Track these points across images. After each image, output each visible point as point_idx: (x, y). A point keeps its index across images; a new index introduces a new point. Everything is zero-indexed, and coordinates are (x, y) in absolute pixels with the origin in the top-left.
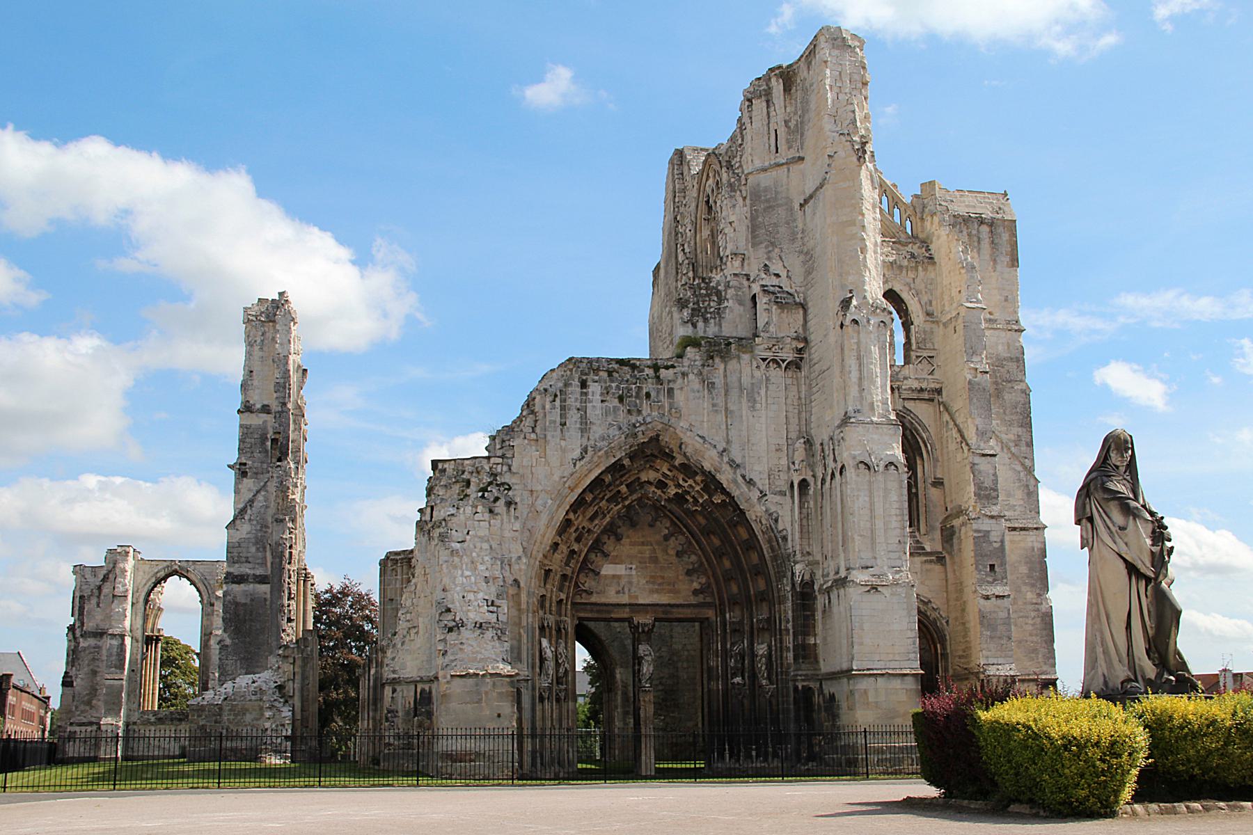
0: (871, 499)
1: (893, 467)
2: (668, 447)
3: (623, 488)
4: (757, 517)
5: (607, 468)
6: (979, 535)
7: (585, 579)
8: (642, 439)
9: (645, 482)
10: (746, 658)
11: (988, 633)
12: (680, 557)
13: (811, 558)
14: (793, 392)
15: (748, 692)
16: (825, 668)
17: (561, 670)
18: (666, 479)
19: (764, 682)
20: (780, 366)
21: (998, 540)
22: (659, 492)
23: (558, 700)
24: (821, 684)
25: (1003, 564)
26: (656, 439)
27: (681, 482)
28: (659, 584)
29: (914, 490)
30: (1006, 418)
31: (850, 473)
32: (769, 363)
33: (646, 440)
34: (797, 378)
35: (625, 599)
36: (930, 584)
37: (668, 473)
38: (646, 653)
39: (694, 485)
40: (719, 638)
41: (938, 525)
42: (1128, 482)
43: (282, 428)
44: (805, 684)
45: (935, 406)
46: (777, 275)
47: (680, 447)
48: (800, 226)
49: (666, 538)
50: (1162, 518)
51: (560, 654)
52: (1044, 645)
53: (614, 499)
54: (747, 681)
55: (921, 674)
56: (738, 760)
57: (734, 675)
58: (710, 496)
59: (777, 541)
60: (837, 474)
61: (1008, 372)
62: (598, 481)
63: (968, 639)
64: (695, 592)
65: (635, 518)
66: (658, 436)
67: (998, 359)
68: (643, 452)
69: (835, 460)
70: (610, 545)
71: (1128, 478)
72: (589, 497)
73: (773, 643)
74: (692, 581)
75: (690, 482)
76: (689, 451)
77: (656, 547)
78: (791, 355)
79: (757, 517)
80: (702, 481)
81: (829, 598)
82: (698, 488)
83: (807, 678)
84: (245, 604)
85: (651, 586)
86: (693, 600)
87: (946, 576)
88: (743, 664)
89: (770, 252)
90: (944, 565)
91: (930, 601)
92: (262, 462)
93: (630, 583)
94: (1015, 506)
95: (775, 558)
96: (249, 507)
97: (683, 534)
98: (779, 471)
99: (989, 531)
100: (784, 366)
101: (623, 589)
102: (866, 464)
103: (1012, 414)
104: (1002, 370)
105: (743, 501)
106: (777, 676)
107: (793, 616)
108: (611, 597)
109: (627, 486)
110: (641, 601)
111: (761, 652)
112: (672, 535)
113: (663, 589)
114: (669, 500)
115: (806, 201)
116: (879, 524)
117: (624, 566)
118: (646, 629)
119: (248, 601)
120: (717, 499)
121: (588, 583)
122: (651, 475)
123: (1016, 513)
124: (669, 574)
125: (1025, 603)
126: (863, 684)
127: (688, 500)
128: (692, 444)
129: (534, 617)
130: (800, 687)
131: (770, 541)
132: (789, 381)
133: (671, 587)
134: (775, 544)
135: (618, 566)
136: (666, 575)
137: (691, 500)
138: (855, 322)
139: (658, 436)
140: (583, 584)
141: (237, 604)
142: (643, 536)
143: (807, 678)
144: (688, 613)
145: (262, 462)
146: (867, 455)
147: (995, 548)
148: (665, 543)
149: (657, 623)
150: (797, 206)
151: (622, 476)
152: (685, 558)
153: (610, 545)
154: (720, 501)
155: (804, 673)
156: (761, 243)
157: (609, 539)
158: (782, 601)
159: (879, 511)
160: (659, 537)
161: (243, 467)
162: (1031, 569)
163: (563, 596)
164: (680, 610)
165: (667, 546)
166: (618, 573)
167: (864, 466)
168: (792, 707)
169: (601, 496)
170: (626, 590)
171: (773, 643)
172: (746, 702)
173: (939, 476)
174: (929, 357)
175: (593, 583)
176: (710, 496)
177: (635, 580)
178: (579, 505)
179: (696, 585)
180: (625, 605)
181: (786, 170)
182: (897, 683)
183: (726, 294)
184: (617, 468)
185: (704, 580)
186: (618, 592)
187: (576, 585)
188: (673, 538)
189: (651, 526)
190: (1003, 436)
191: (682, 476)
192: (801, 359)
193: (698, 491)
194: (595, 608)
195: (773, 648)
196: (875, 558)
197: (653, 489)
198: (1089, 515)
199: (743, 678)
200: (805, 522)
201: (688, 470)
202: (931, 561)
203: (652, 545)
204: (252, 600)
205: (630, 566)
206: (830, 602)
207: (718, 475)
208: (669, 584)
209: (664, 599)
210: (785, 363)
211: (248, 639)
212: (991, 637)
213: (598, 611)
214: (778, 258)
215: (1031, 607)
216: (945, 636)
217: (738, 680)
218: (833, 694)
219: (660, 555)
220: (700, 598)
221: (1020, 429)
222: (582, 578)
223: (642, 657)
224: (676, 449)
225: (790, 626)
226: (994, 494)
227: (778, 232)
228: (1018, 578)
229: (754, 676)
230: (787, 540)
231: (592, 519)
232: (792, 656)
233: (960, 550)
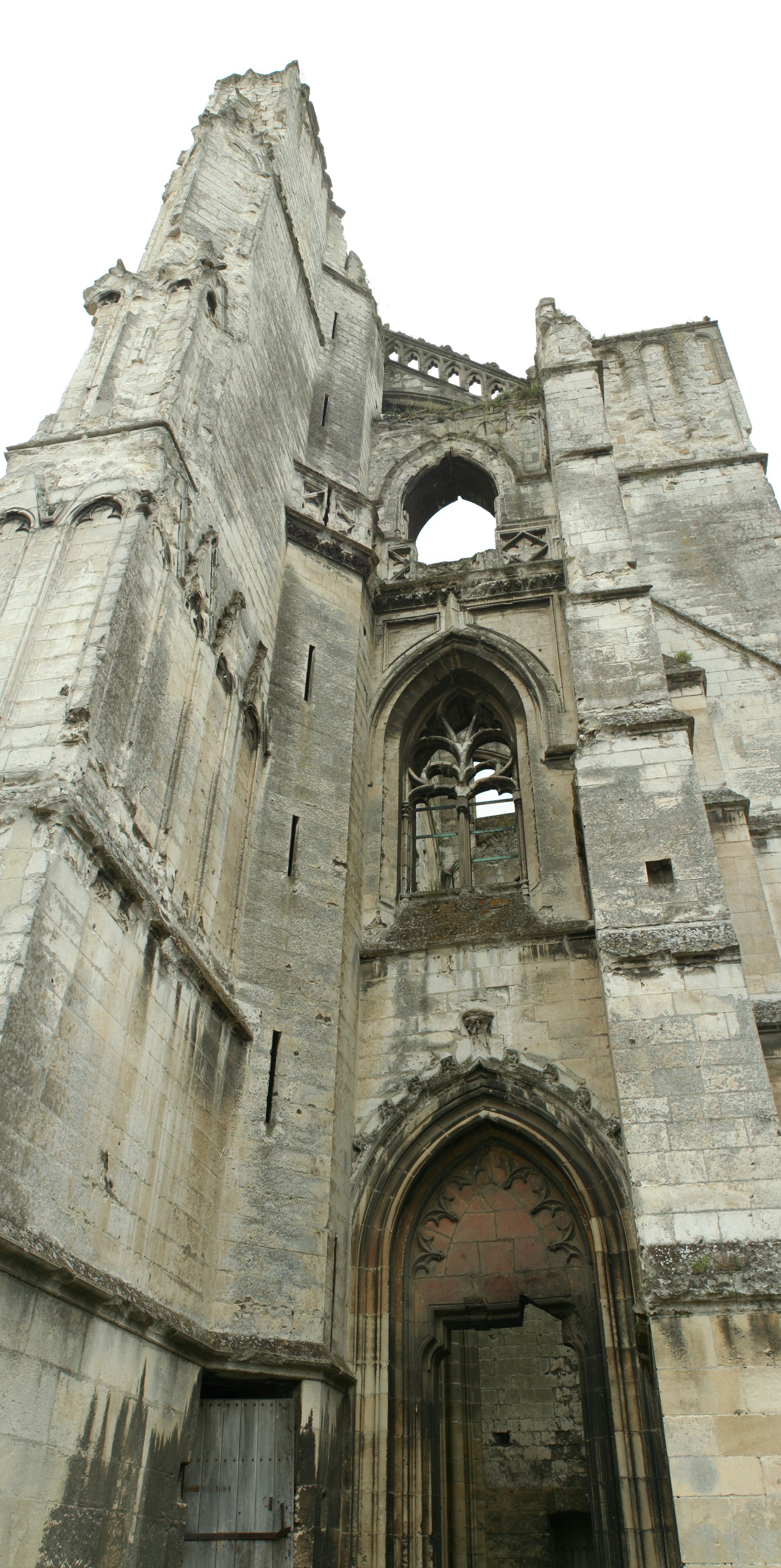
6: (603, 782)
11: (661, 1105)
21: (675, 786)
30: (749, 606)
61: (739, 527)
91: (552, 1071)
99: (634, 770)
104: (723, 527)
212: (672, 1121)
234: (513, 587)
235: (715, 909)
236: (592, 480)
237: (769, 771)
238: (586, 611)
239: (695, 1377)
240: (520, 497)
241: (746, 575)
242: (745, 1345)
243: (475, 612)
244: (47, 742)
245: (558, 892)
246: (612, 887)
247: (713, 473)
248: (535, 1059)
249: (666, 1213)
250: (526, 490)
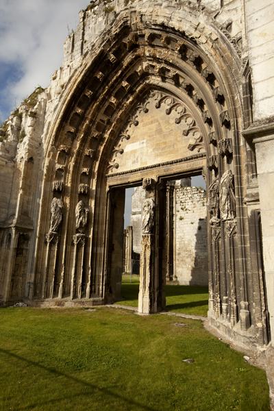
4: (206, 37)
8: (115, 30)
26: (125, 29)
28: (163, 149)
47: (142, 21)
53: (122, 94)
64: (193, 148)
77: (161, 121)
93: (142, 153)
101: (137, 159)
105: (192, 31)
109: (127, 81)
113: (166, 152)
133: (172, 149)
135: (135, 144)
136: (167, 140)
160: (164, 113)
164: (178, 165)
170: (139, 159)
179: (192, 142)
184: (100, 62)
186: (134, 162)
203: (157, 121)
220: (195, 152)
224: (141, 25)
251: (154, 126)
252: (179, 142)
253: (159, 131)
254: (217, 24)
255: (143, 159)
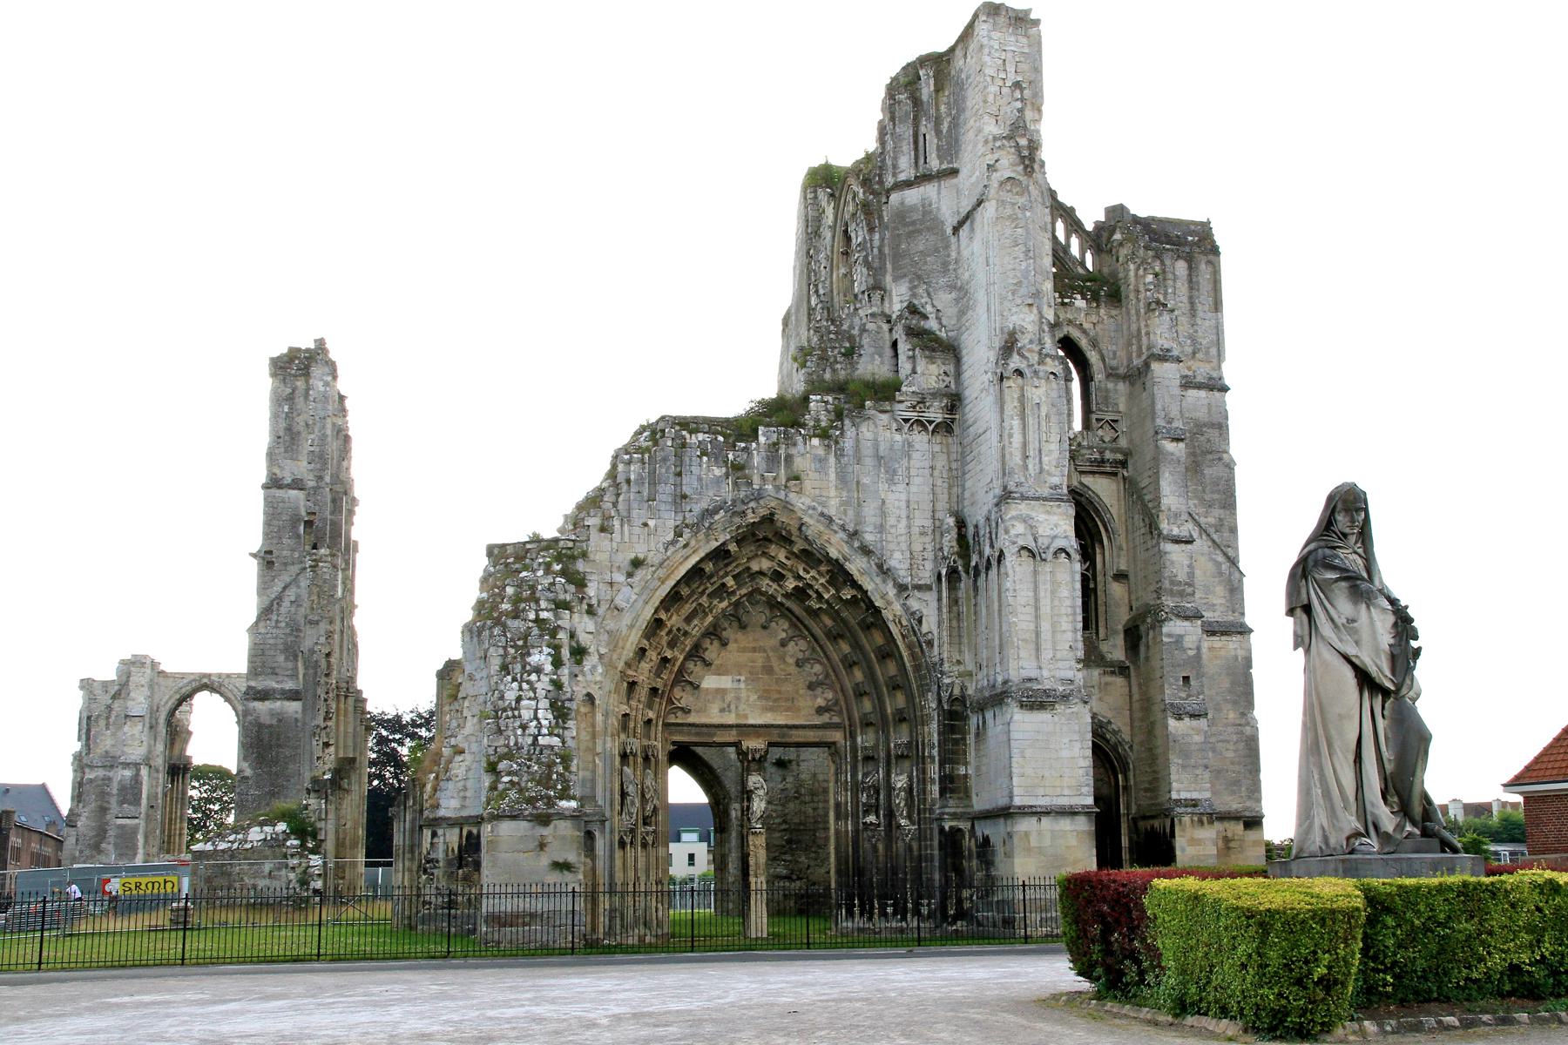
0: (1035, 594)
1: (1063, 555)
2: (785, 529)
3: (730, 582)
5: (707, 555)
7: (682, 694)
8: (751, 518)
9: (757, 572)
10: (881, 791)
11: (1180, 761)
12: (800, 667)
13: (962, 668)
14: (941, 462)
15: (883, 833)
16: (979, 803)
17: (649, 807)
18: (783, 568)
19: (903, 822)
20: (926, 429)
21: (1194, 647)
22: (775, 586)
23: (644, 845)
24: (973, 825)
25: (1200, 676)
26: (769, 519)
27: (801, 573)
28: (775, 700)
29: (1092, 586)
30: (1206, 497)
31: (1010, 559)
32: (912, 425)
33: (756, 520)
34: (948, 445)
35: (731, 719)
36: (1113, 700)
37: (784, 561)
38: (757, 785)
39: (817, 576)
40: (849, 767)
41: (1120, 628)
42: (1360, 556)
43: (317, 508)
44: (953, 824)
45: (1118, 483)
46: (925, 317)
47: (800, 529)
48: (954, 255)
49: (783, 644)
50: (1406, 607)
51: (648, 787)
52: (1248, 775)
53: (722, 591)
54: (882, 821)
55: (1097, 813)
56: (870, 919)
57: (866, 813)
58: (838, 591)
59: (921, 646)
60: (994, 563)
61: (1209, 440)
62: (696, 573)
63: (1155, 768)
64: (820, 711)
65: (744, 619)
66: (772, 514)
67: (1197, 425)
68: (754, 535)
69: (992, 546)
70: (712, 651)
71: (1360, 551)
72: (685, 591)
73: (915, 774)
74: (816, 697)
75: (813, 573)
76: (809, 533)
77: (771, 654)
78: (939, 415)
79: (895, 616)
80: (828, 572)
81: (984, 718)
82: (822, 581)
83: (955, 816)
84: (271, 726)
85: (764, 703)
86: (818, 721)
87: (1130, 691)
88: (877, 799)
89: (915, 287)
90: (1128, 677)
91: (1109, 722)
92: (293, 550)
93: (738, 699)
94: (1214, 605)
95: (917, 668)
96: (275, 606)
97: (805, 638)
98: (924, 560)
99: (1181, 636)
100: (931, 428)
101: (729, 706)
102: (1030, 551)
103: (1212, 492)
104: (1202, 438)
105: (878, 597)
106: (919, 814)
107: (939, 740)
108: (714, 716)
109: (734, 577)
110: (751, 721)
111: (899, 785)
112: (791, 639)
114: (787, 596)
115: (961, 224)
116: (1045, 626)
117: (730, 678)
118: (757, 756)
119: (274, 722)
120: (847, 594)
121: (684, 697)
122: (765, 564)
123: (1216, 614)
124: (788, 688)
125: (1226, 725)
126: (1024, 825)
127: (810, 596)
128: (814, 527)
129: (614, 741)
130: (947, 828)
131: (910, 647)
132: (937, 448)
133: (789, 704)
134: (917, 650)
135: (723, 677)
136: (783, 689)
137: (814, 596)
138: (1019, 373)
139: (772, 514)
140: (679, 700)
141: (260, 726)
142: (755, 640)
143: (955, 816)
144: (811, 736)
145: (293, 550)
146: (1031, 538)
147: (1189, 657)
148: (782, 649)
149: (770, 749)
150: (949, 231)
151: (727, 565)
152: (807, 667)
153: (712, 651)
154: (849, 597)
155: (952, 810)
156: (905, 276)
157: (711, 644)
158: (924, 721)
159: (1045, 608)
160: (774, 642)
161: (269, 556)
162: (1232, 683)
163: (651, 715)
164: (801, 732)
165: (785, 653)
166: (722, 687)
167: (1027, 554)
168: (936, 852)
169: (700, 590)
170: (733, 707)
171: (915, 774)
172: (881, 847)
173: (1123, 567)
174: (1112, 421)
175: (691, 699)
176: (838, 591)
177: (744, 695)
178: (673, 599)
179: (820, 702)
180: (730, 726)
181: (936, 188)
182: (1065, 824)
183: (861, 339)
185: (830, 695)
186: (722, 710)
187: (670, 701)
188: (792, 643)
189: (764, 627)
190: (1202, 520)
191: (803, 565)
192: (953, 421)
193: (822, 584)
194: (693, 730)
195: (915, 780)
196: (1040, 668)
197: (767, 581)
198: (1306, 602)
199: (878, 817)
200: (955, 623)
201: (811, 556)
202: (1113, 673)
203: (765, 651)
204: (280, 721)
205: (738, 678)
206: (984, 722)
207: (847, 563)
208: (787, 700)
209: (780, 720)
210: (934, 425)
211: (274, 769)
212: (1184, 767)
213: (697, 734)
214: (925, 295)
215: (1230, 729)
216: (1128, 763)
217: (871, 818)
218: (988, 836)
219: (775, 663)
220: (825, 718)
221: (1222, 511)
222: (677, 692)
223: (751, 791)
224: (795, 532)
225: (935, 752)
226: (1189, 590)
227: (926, 263)
228: (1217, 694)
229: (890, 815)
230: (932, 646)
231: (688, 620)
232: (937, 789)
233: (1147, 659)
234: (1102, 462)
235: (1201, 697)
236: (1174, 458)
237: (1201, 598)
238: (1168, 547)
239: (1183, 830)
240: (1107, 391)
241: (1207, 477)
242: (1196, 824)
243: (1082, 473)
244: (1071, 668)
245: (1114, 646)
246: (1171, 684)
247: (1203, 393)
248: (1104, 717)
249: (1178, 791)
250: (1110, 386)
251: (759, 658)
252: (801, 696)
253: (768, 670)
254: (908, 609)
255: (740, 708)
